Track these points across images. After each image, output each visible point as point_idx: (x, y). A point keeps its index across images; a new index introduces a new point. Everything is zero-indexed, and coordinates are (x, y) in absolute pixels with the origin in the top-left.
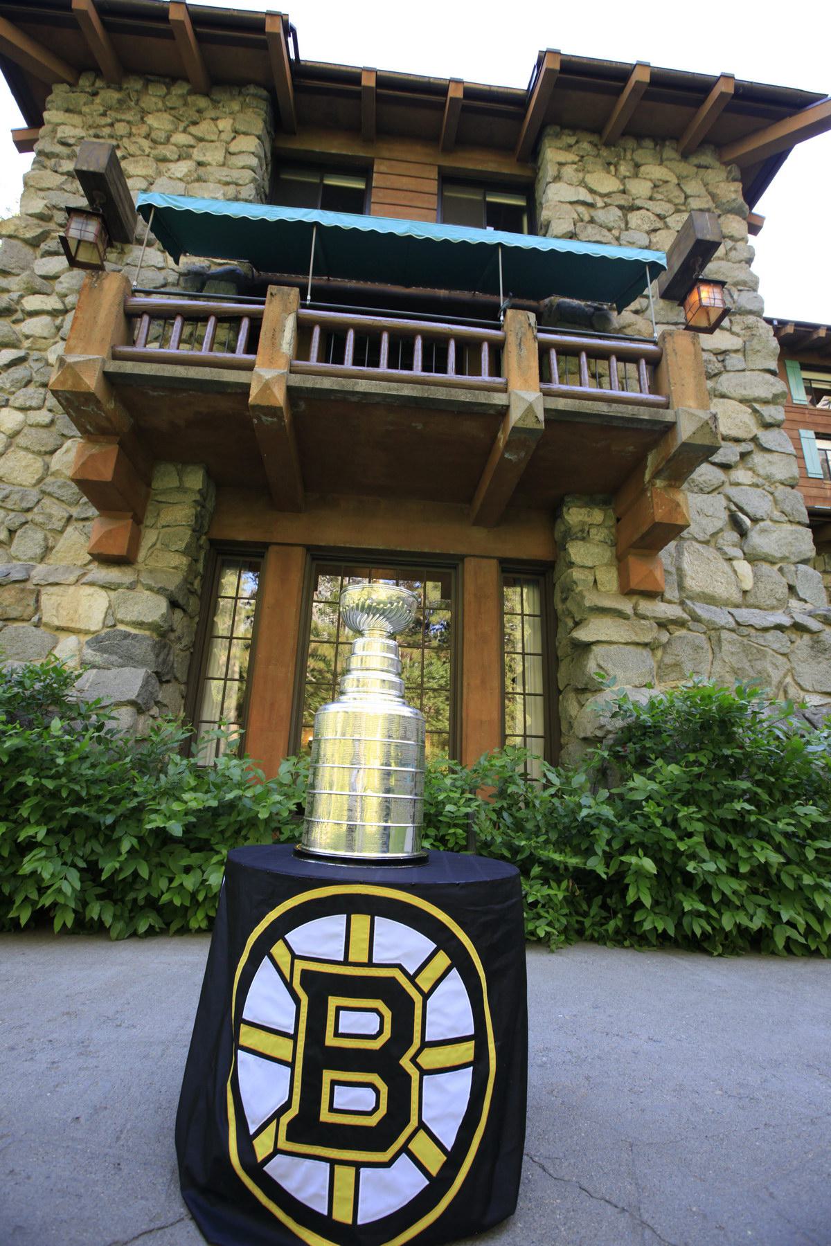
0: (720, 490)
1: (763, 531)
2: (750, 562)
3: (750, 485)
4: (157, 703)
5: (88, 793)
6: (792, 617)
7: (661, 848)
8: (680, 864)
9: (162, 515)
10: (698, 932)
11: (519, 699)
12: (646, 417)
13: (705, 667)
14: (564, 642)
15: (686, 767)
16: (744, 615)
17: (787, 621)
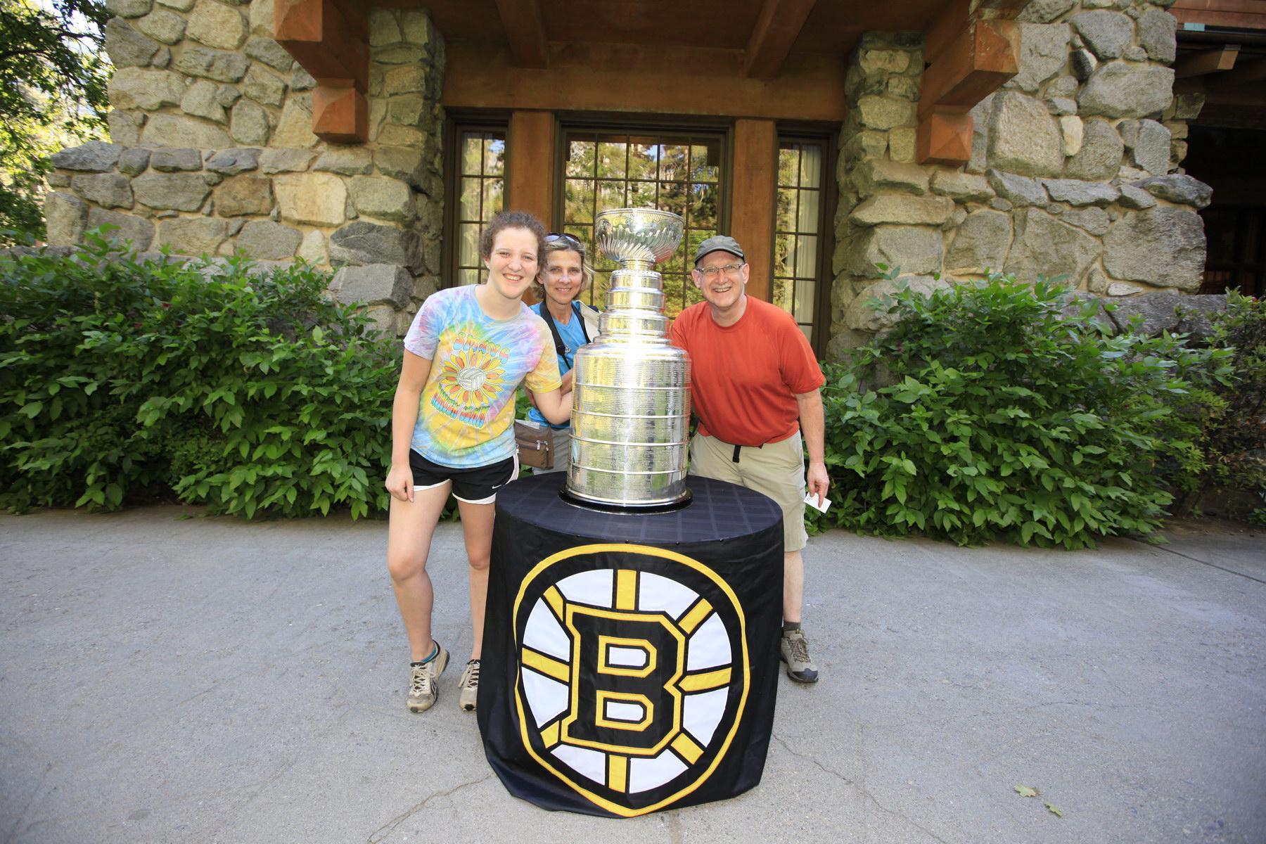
0: (1067, 16)
1: (1110, 74)
2: (1082, 118)
3: (1108, 8)
4: (413, 298)
5: (360, 400)
6: (1120, 190)
7: (923, 450)
8: (940, 465)
9: (388, 81)
10: (947, 526)
11: (788, 285)
13: (1002, 252)
14: (844, 221)
15: (964, 371)
16: (1062, 188)
17: (1110, 194)
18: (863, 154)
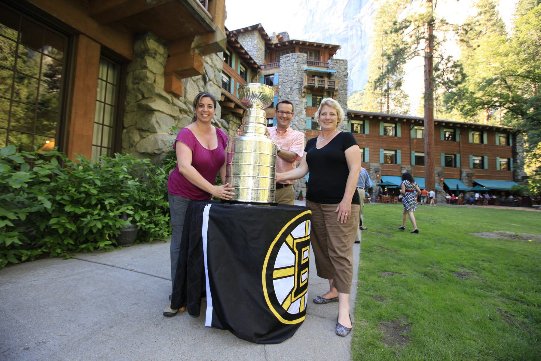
1: (210, 85)
12: (208, 22)
18: (146, 79)
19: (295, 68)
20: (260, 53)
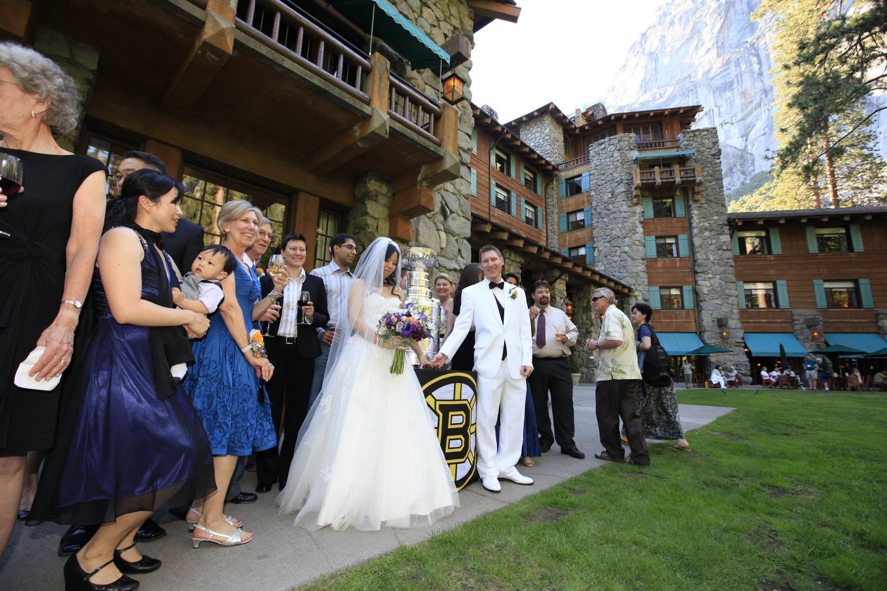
1: (453, 219)
6: (460, 266)
19: (616, 159)
20: (556, 147)
